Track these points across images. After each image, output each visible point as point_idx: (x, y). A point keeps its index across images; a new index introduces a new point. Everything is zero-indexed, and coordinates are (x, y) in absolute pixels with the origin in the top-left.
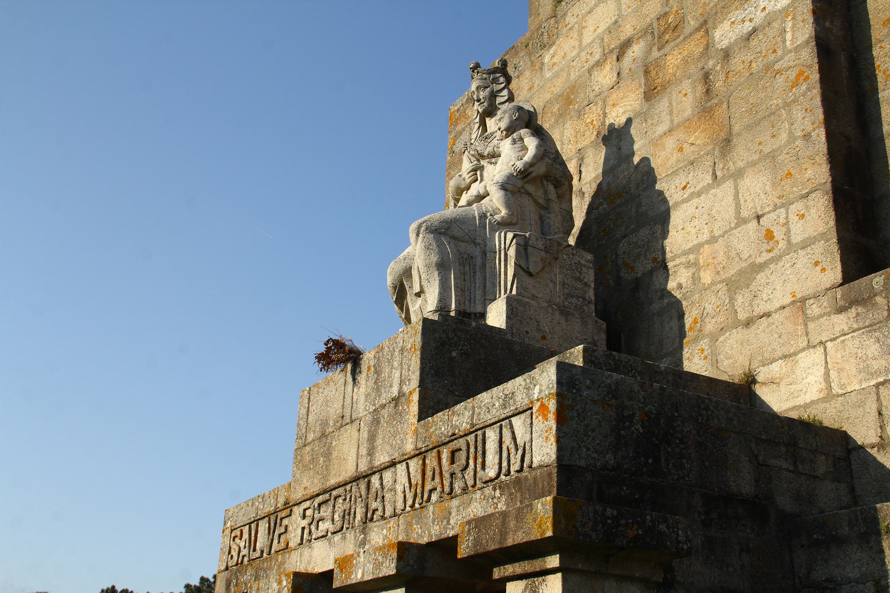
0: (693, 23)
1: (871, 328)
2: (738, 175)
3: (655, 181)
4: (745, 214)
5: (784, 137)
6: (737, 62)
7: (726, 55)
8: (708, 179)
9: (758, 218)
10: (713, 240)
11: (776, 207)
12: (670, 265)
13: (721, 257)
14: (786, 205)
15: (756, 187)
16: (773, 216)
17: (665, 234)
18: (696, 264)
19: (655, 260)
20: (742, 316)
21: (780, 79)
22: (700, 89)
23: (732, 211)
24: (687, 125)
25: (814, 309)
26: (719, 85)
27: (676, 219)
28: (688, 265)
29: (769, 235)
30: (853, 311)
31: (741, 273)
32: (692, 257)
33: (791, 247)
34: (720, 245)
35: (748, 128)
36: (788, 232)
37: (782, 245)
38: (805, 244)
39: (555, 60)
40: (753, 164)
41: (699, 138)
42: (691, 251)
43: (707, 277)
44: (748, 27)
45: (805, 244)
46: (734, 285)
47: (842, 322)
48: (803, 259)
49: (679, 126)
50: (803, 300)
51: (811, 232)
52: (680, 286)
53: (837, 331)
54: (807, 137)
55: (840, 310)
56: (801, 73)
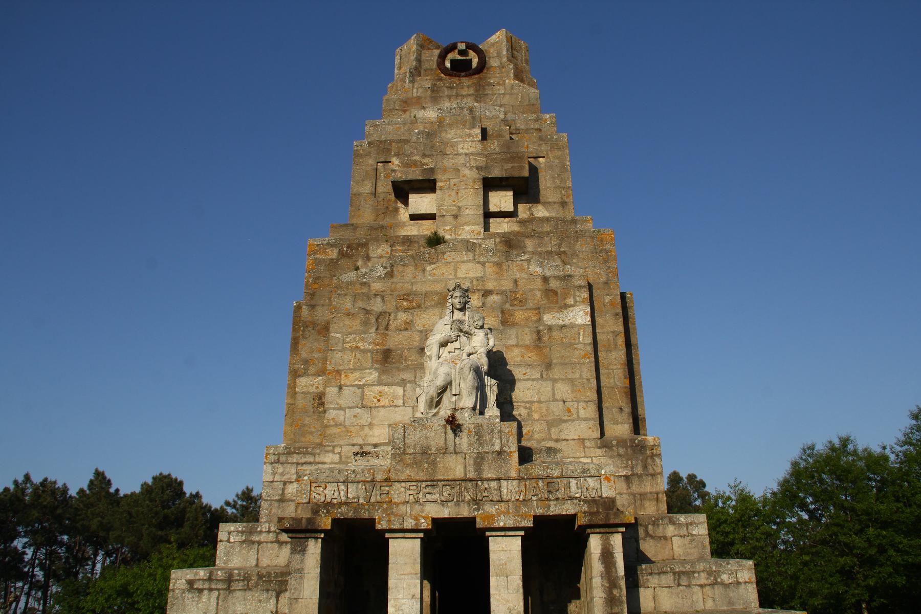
0: (530, 304)
1: (611, 457)
2: (555, 381)
3: (507, 364)
4: (557, 397)
5: (577, 376)
6: (555, 334)
7: (550, 328)
8: (538, 376)
9: (564, 402)
10: (539, 402)
11: (572, 401)
12: (515, 404)
13: (544, 410)
14: (578, 402)
15: (563, 390)
16: (571, 403)
17: (513, 390)
18: (530, 408)
19: (506, 399)
20: (554, 437)
21: (577, 352)
22: (535, 336)
23: (550, 394)
24: (527, 347)
25: (588, 444)
26: (545, 338)
27: (518, 386)
28: (525, 408)
29: (569, 410)
30: (604, 450)
31: (554, 420)
32: (528, 405)
33: (578, 418)
34: (543, 405)
35: (561, 364)
36: (578, 412)
37: (575, 416)
38: (585, 419)
39: (435, 272)
40: (563, 380)
41: (532, 357)
42: (527, 402)
43: (536, 416)
44: (561, 323)
45: (585, 419)
46: (550, 424)
47: (599, 452)
48: (584, 425)
49: (521, 346)
50: (584, 440)
51: (588, 416)
52: (520, 415)
53: (597, 454)
54: (588, 380)
55: (599, 448)
56: (586, 355)
